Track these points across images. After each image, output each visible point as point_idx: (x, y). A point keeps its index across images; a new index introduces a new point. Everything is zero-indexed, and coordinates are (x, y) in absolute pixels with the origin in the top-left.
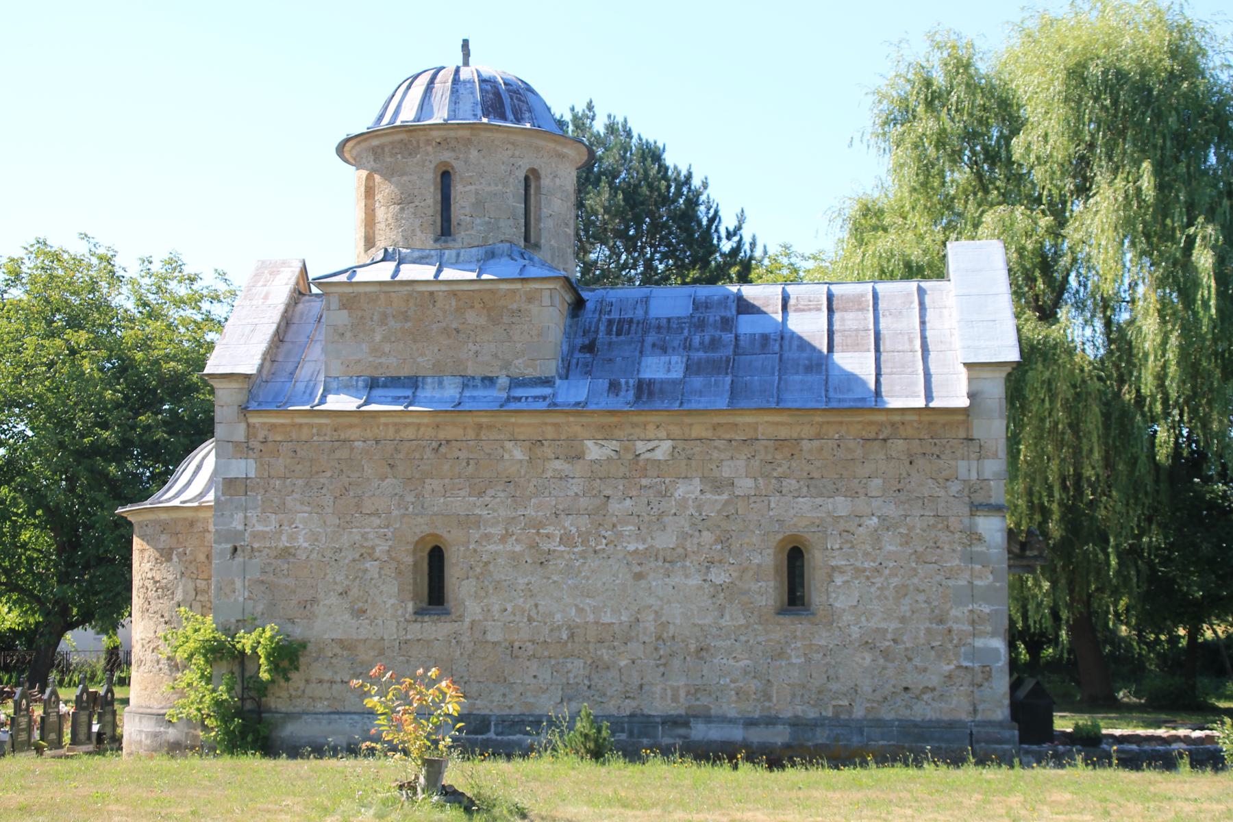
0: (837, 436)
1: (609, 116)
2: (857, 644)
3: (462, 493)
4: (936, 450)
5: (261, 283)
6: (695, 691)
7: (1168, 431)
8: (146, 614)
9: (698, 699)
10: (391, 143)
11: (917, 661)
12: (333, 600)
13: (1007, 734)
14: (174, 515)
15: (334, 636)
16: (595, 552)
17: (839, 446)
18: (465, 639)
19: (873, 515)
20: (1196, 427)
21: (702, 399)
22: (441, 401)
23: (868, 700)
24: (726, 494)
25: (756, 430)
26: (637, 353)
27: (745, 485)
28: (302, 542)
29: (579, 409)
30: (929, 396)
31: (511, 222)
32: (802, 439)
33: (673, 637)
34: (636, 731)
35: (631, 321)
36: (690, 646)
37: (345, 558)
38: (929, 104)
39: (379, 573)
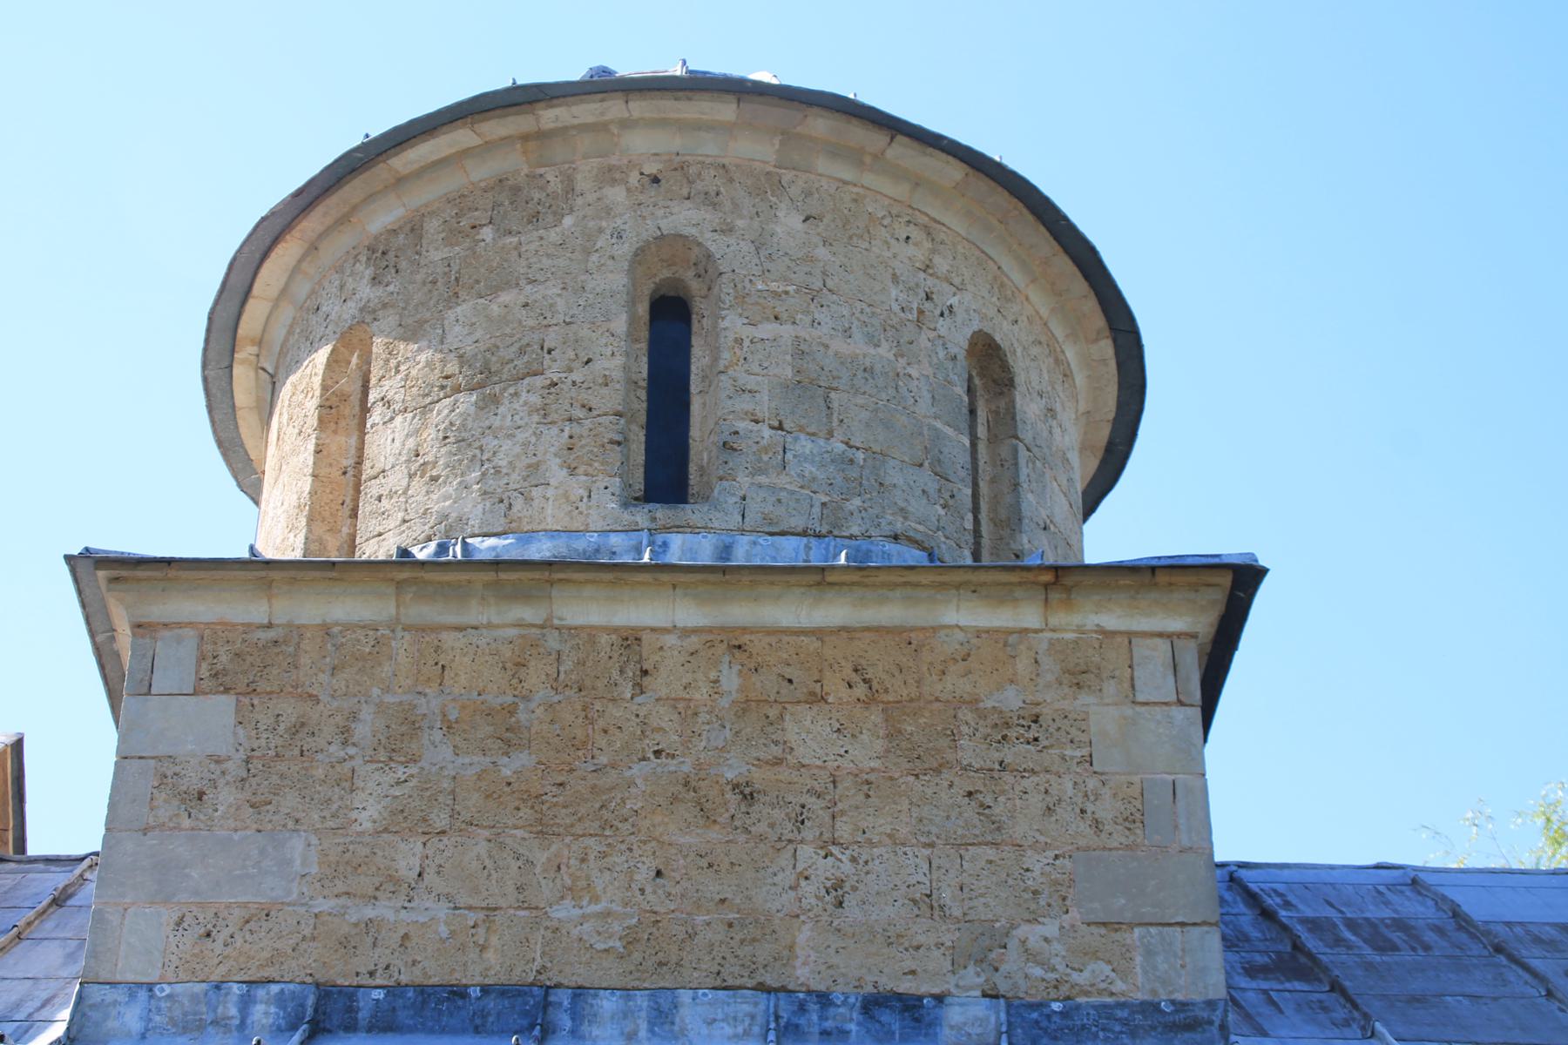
31: (926, 479)
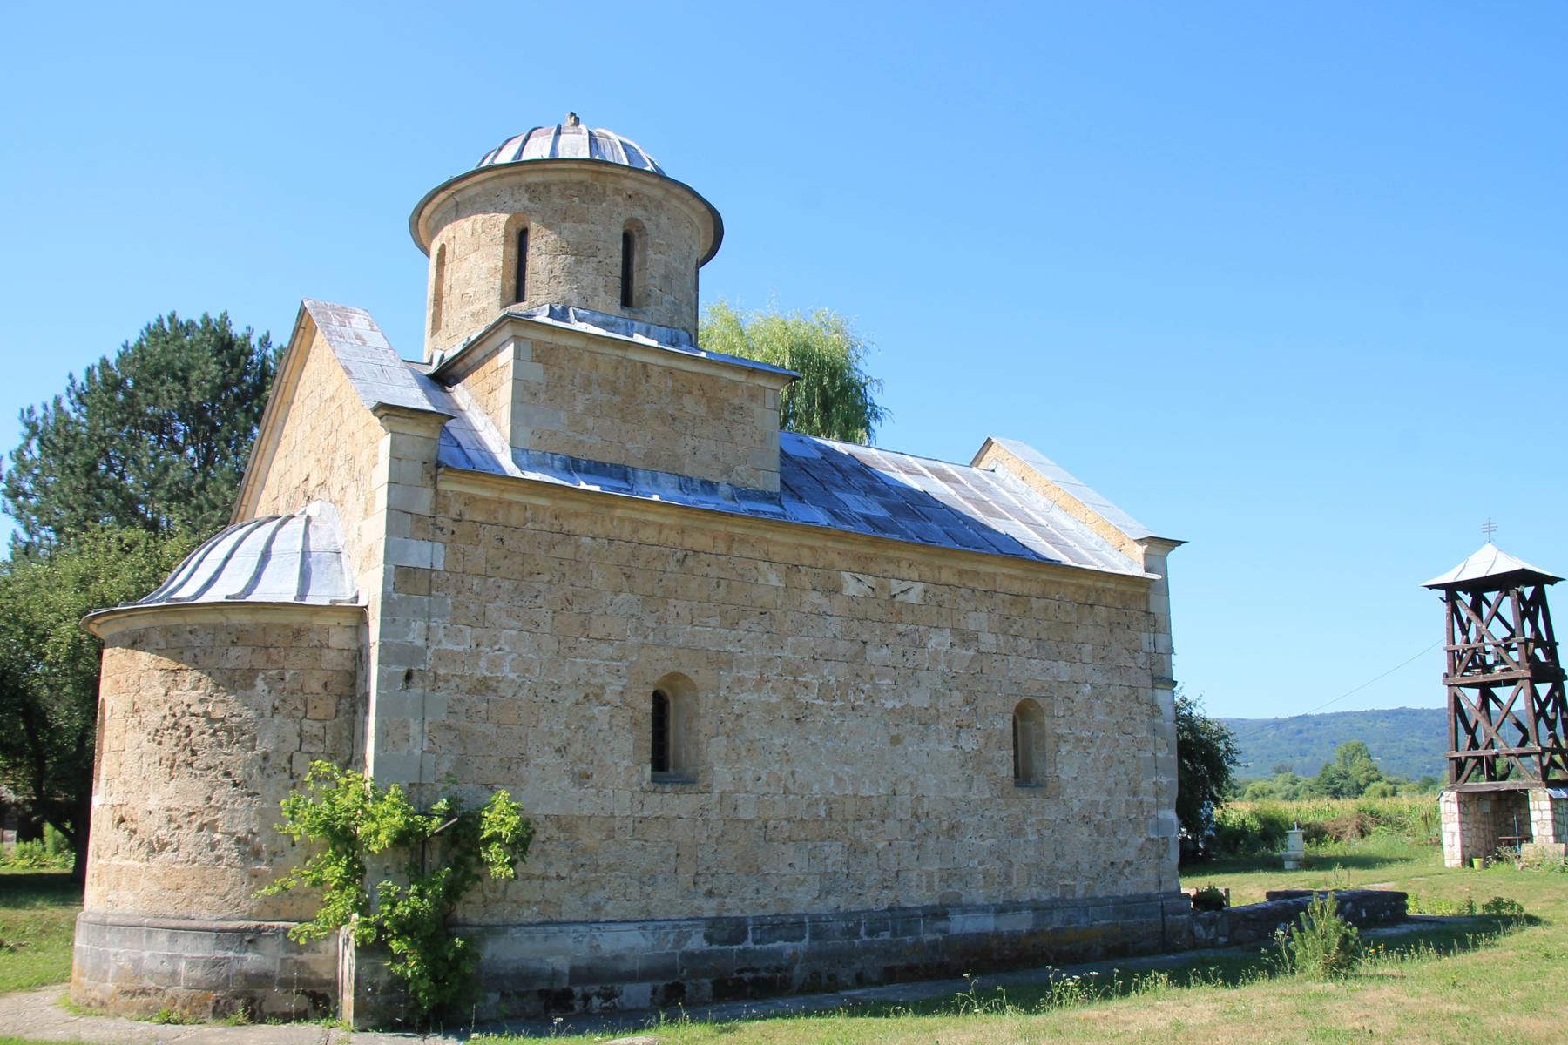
3: (713, 622)
6: (948, 876)
9: (949, 886)
11: (1120, 835)
12: (550, 758)
14: (264, 618)
15: (549, 812)
18: (713, 816)
24: (972, 650)
27: (988, 641)
28: (508, 672)
33: (927, 814)
39: (610, 723)
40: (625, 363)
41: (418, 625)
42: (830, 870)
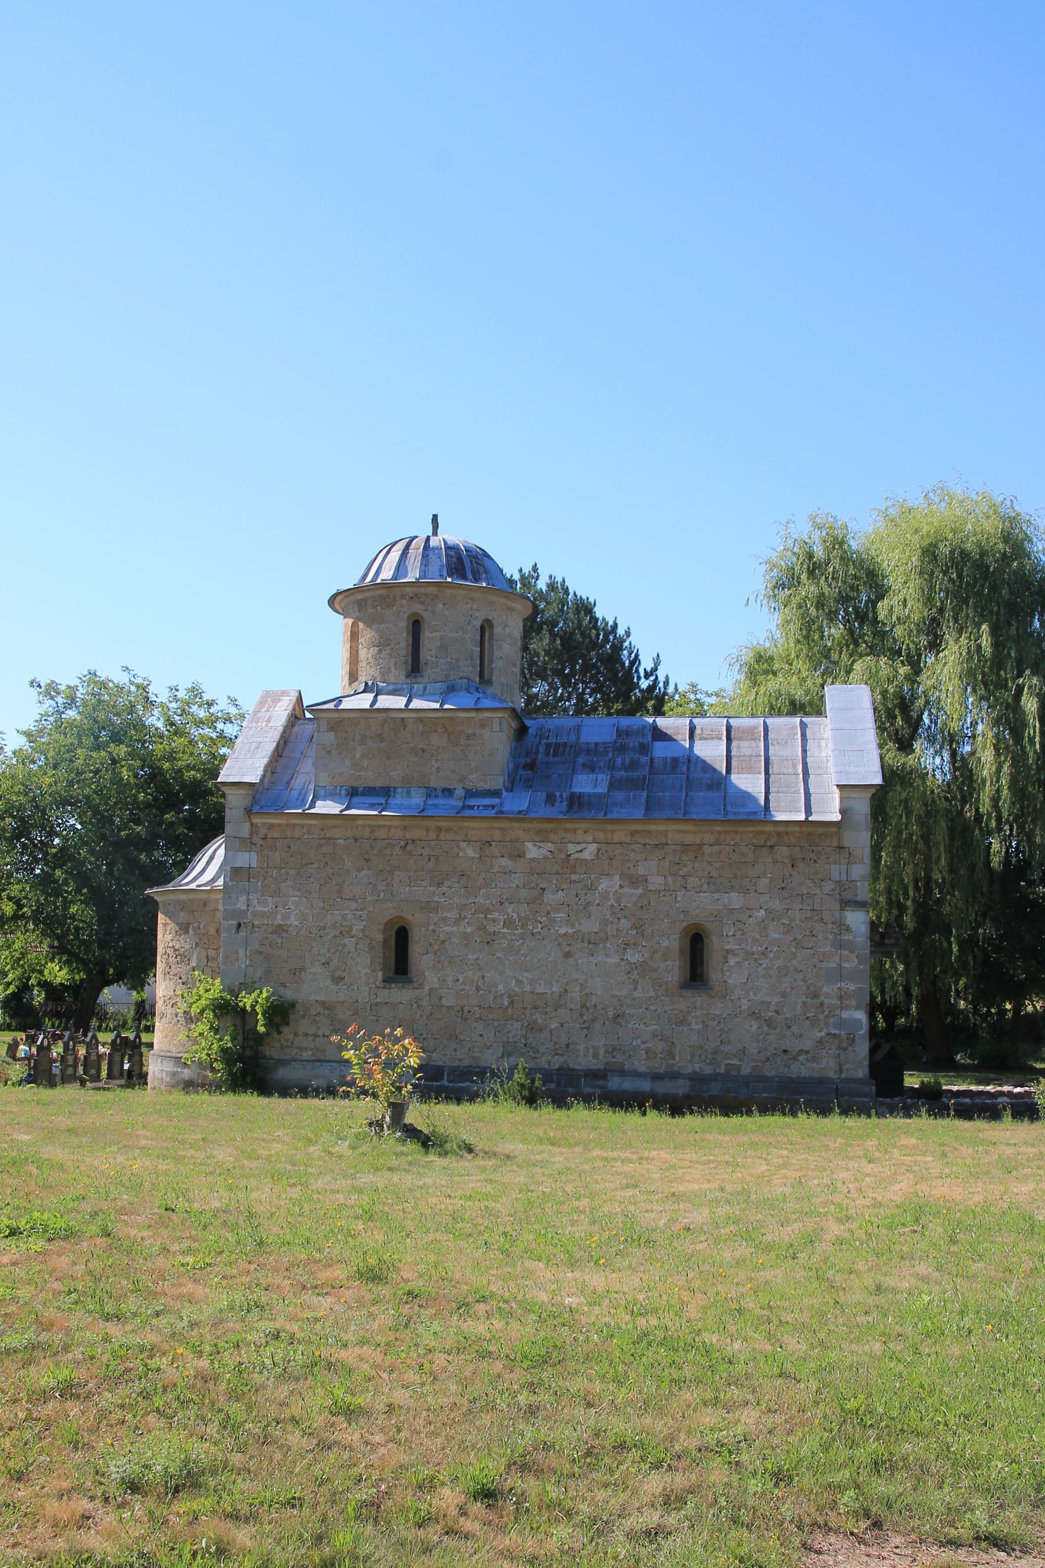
0: (732, 843)
1: (550, 577)
2: (746, 1015)
3: (424, 883)
4: (813, 856)
5: (264, 710)
6: (612, 1050)
7: (1001, 843)
8: (168, 976)
9: (614, 1057)
10: (373, 597)
11: (795, 1029)
12: (318, 969)
13: (866, 1089)
14: (191, 896)
16: (533, 934)
17: (734, 851)
18: (424, 1003)
19: (761, 908)
20: (1022, 839)
21: (623, 810)
22: (409, 807)
23: (754, 1060)
24: (641, 888)
25: (666, 836)
26: (570, 771)
28: (293, 921)
29: (521, 816)
30: (808, 811)
32: (704, 845)
33: (595, 1006)
34: (563, 1082)
35: (565, 745)
36: (609, 1013)
37: (328, 934)
38: (811, 573)
40: (389, 720)
41: (243, 899)
42: (511, 1040)
